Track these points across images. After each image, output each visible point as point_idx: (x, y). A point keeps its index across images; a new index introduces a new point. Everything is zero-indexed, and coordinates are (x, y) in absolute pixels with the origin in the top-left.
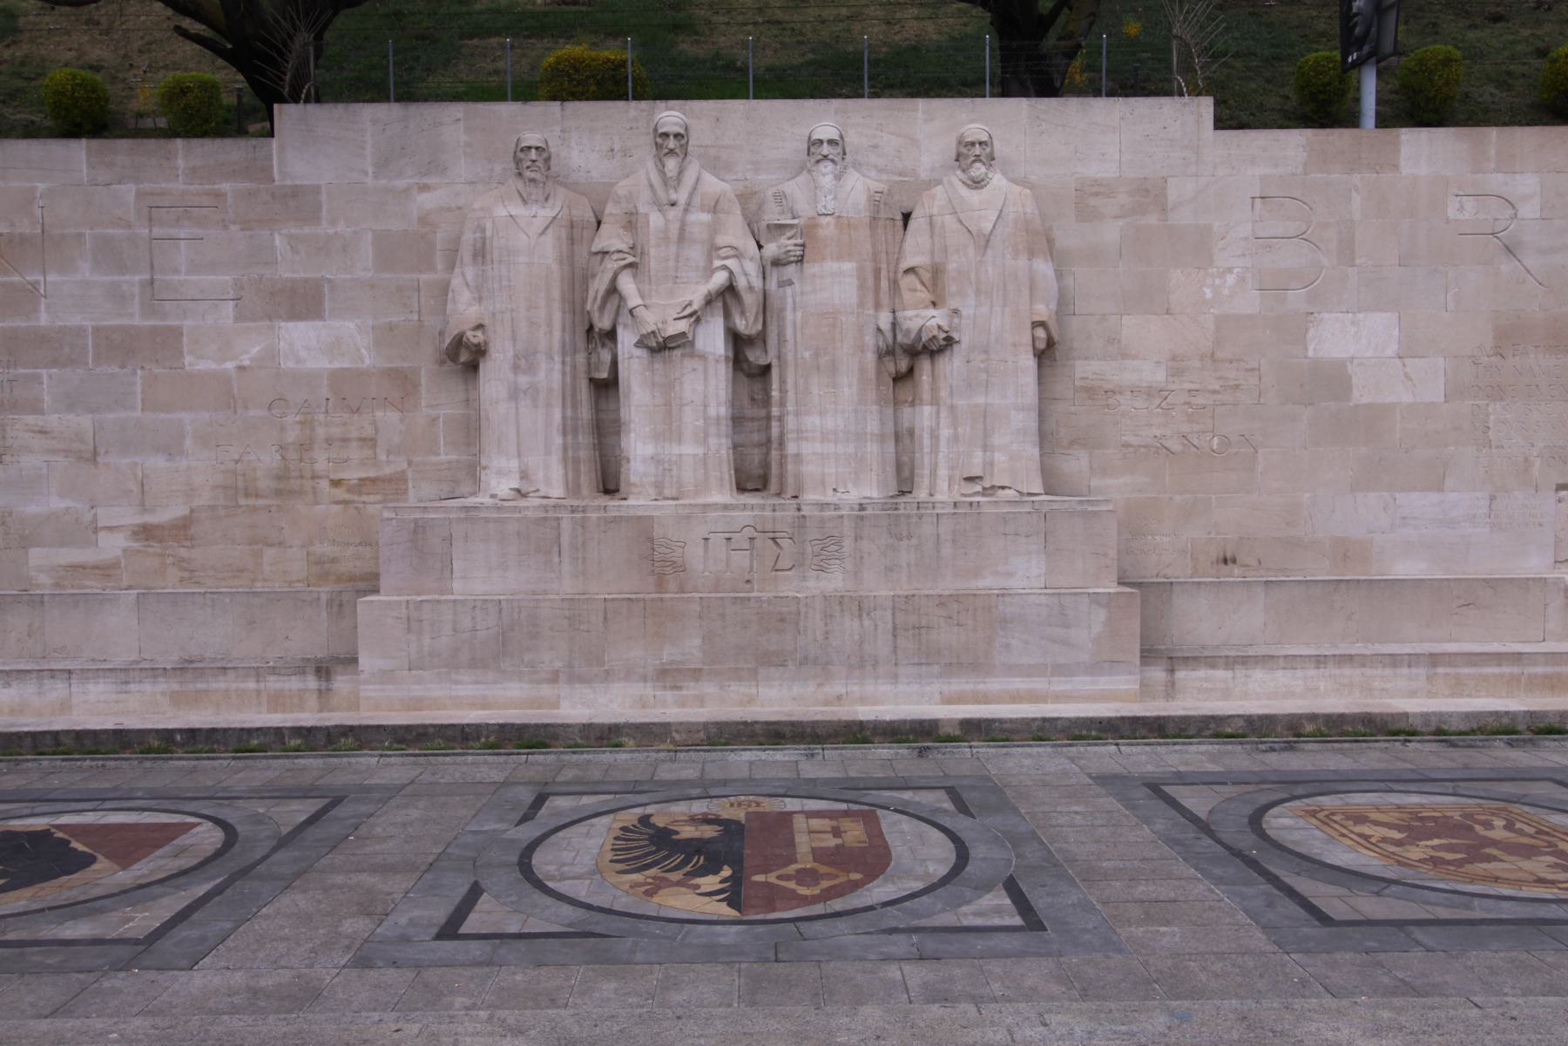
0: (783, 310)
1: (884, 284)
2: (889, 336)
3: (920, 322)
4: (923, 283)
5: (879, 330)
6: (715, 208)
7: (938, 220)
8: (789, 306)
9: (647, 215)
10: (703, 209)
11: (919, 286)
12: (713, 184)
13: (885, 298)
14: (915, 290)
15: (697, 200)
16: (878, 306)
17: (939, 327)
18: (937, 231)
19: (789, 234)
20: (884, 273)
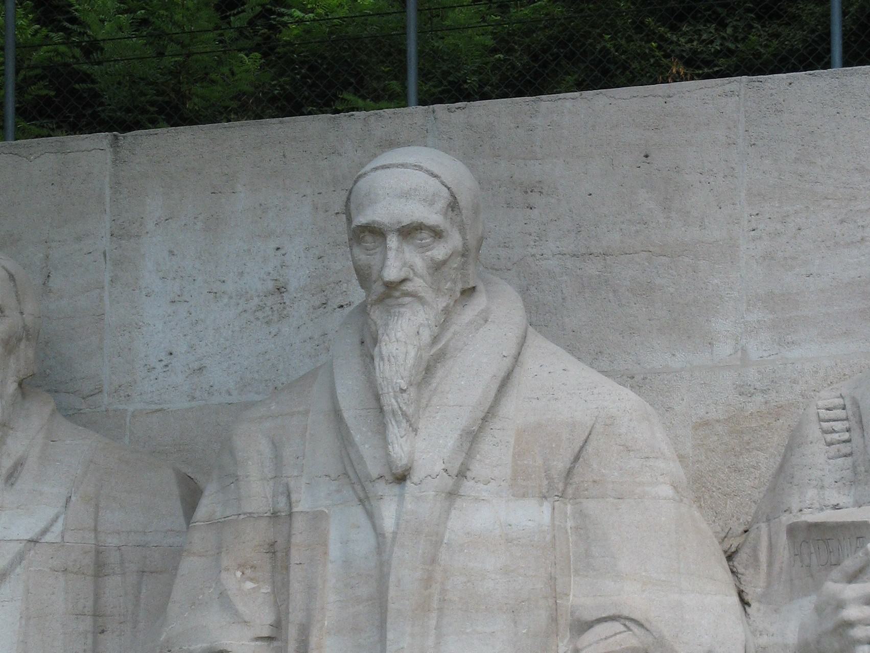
6: (568, 475)
9: (317, 518)
10: (519, 486)
12: (566, 389)
15: (496, 455)
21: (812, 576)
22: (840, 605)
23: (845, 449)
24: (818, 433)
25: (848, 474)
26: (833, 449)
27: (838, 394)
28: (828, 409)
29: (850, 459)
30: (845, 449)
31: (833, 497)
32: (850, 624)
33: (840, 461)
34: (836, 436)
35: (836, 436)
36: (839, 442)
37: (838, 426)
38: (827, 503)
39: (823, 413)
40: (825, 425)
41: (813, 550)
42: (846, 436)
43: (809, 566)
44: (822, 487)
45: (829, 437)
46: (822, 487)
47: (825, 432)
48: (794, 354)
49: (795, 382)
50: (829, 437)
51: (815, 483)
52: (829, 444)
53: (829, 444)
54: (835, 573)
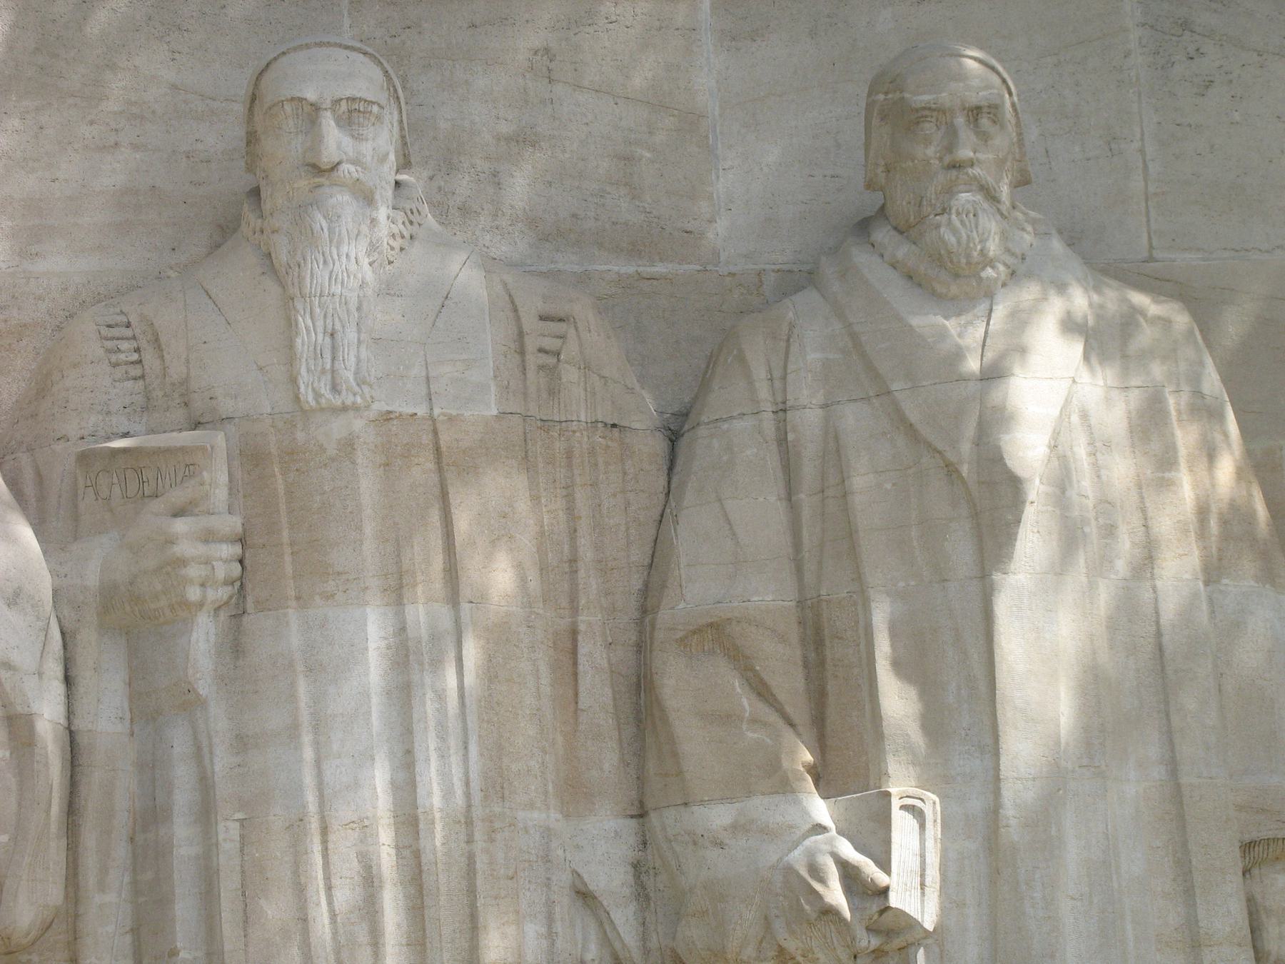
0: (152, 814)
1: (597, 692)
2: (624, 919)
3: (771, 854)
4: (762, 691)
5: (584, 896)
7: (808, 421)
8: (183, 797)
11: (747, 703)
13: (606, 760)
14: (728, 719)
16: (574, 793)
17: (850, 875)
18: (808, 471)
19: (178, 496)
20: (592, 653)
21: (111, 510)
22: (171, 541)
23: (136, 371)
24: (101, 352)
25: (140, 399)
26: (119, 372)
27: (118, 310)
28: (109, 326)
29: (141, 382)
30: (136, 371)
31: (123, 423)
32: (182, 562)
33: (130, 384)
34: (122, 357)
35: (122, 357)
36: (127, 363)
37: (125, 345)
38: (115, 430)
39: (105, 331)
40: (109, 344)
41: (115, 480)
42: (135, 357)
43: (108, 499)
44: (108, 413)
45: (114, 358)
46: (108, 413)
47: (109, 351)
48: (40, 266)
49: (40, 298)
50: (114, 358)
51: (100, 408)
52: (115, 365)
53: (115, 365)
54: (157, 505)
